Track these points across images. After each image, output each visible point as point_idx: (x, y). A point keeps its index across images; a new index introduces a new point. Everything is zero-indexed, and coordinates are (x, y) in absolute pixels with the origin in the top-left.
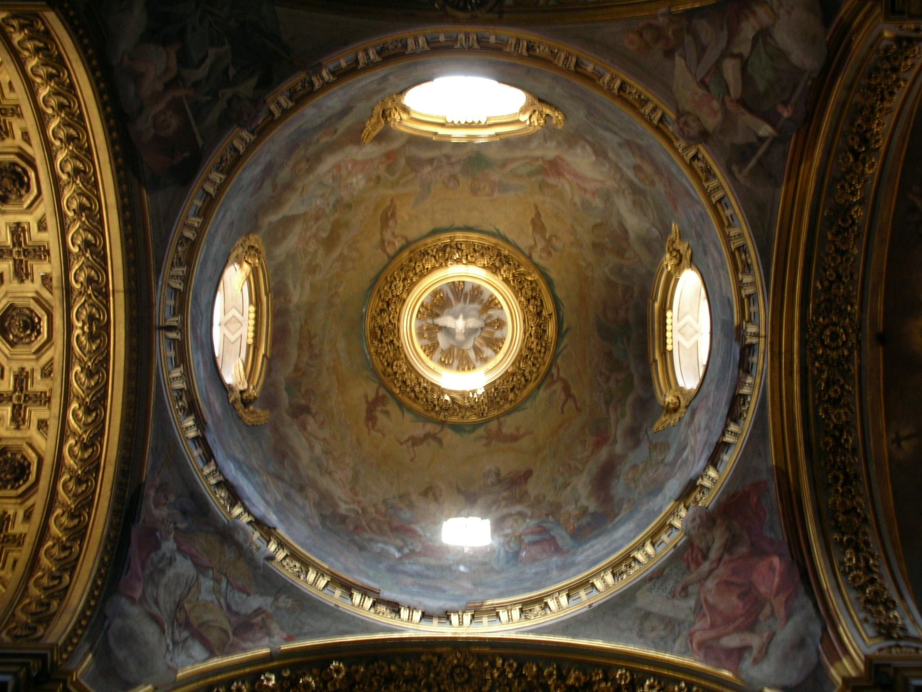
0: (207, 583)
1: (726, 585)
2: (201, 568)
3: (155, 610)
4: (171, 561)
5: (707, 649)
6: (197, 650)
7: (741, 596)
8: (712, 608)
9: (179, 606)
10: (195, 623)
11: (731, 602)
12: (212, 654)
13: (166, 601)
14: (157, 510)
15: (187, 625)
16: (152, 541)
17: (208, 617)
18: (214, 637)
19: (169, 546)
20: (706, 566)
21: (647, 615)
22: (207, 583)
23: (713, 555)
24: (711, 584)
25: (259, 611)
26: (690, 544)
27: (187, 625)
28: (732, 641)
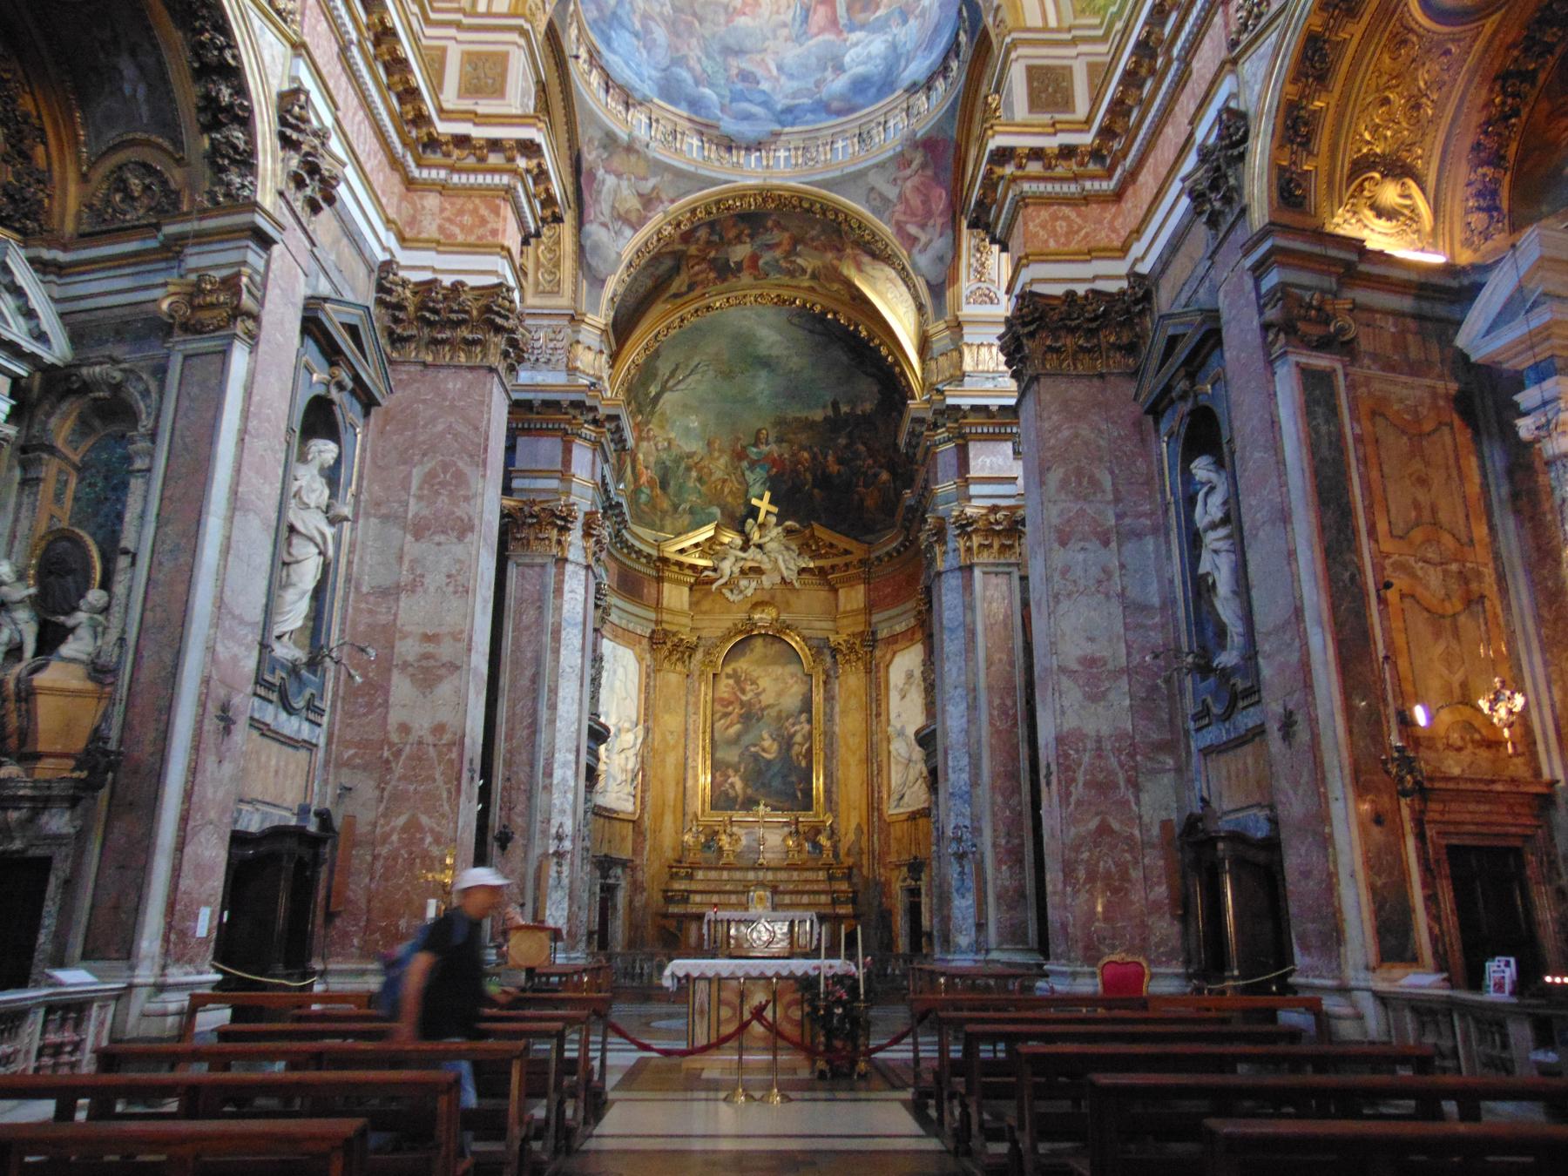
0: (624, 184)
1: (917, 189)
2: (619, 176)
3: (602, 219)
4: (603, 181)
5: (900, 229)
6: (628, 232)
7: (923, 203)
8: (907, 201)
9: (613, 207)
10: (622, 212)
11: (916, 201)
12: (636, 231)
13: (605, 207)
14: (590, 156)
15: (620, 217)
16: (592, 176)
17: (628, 206)
18: (633, 217)
19: (600, 173)
20: (908, 172)
21: (873, 189)
22: (624, 184)
23: (914, 165)
24: (909, 184)
25: (654, 188)
26: (902, 154)
27: (620, 217)
28: (912, 229)
